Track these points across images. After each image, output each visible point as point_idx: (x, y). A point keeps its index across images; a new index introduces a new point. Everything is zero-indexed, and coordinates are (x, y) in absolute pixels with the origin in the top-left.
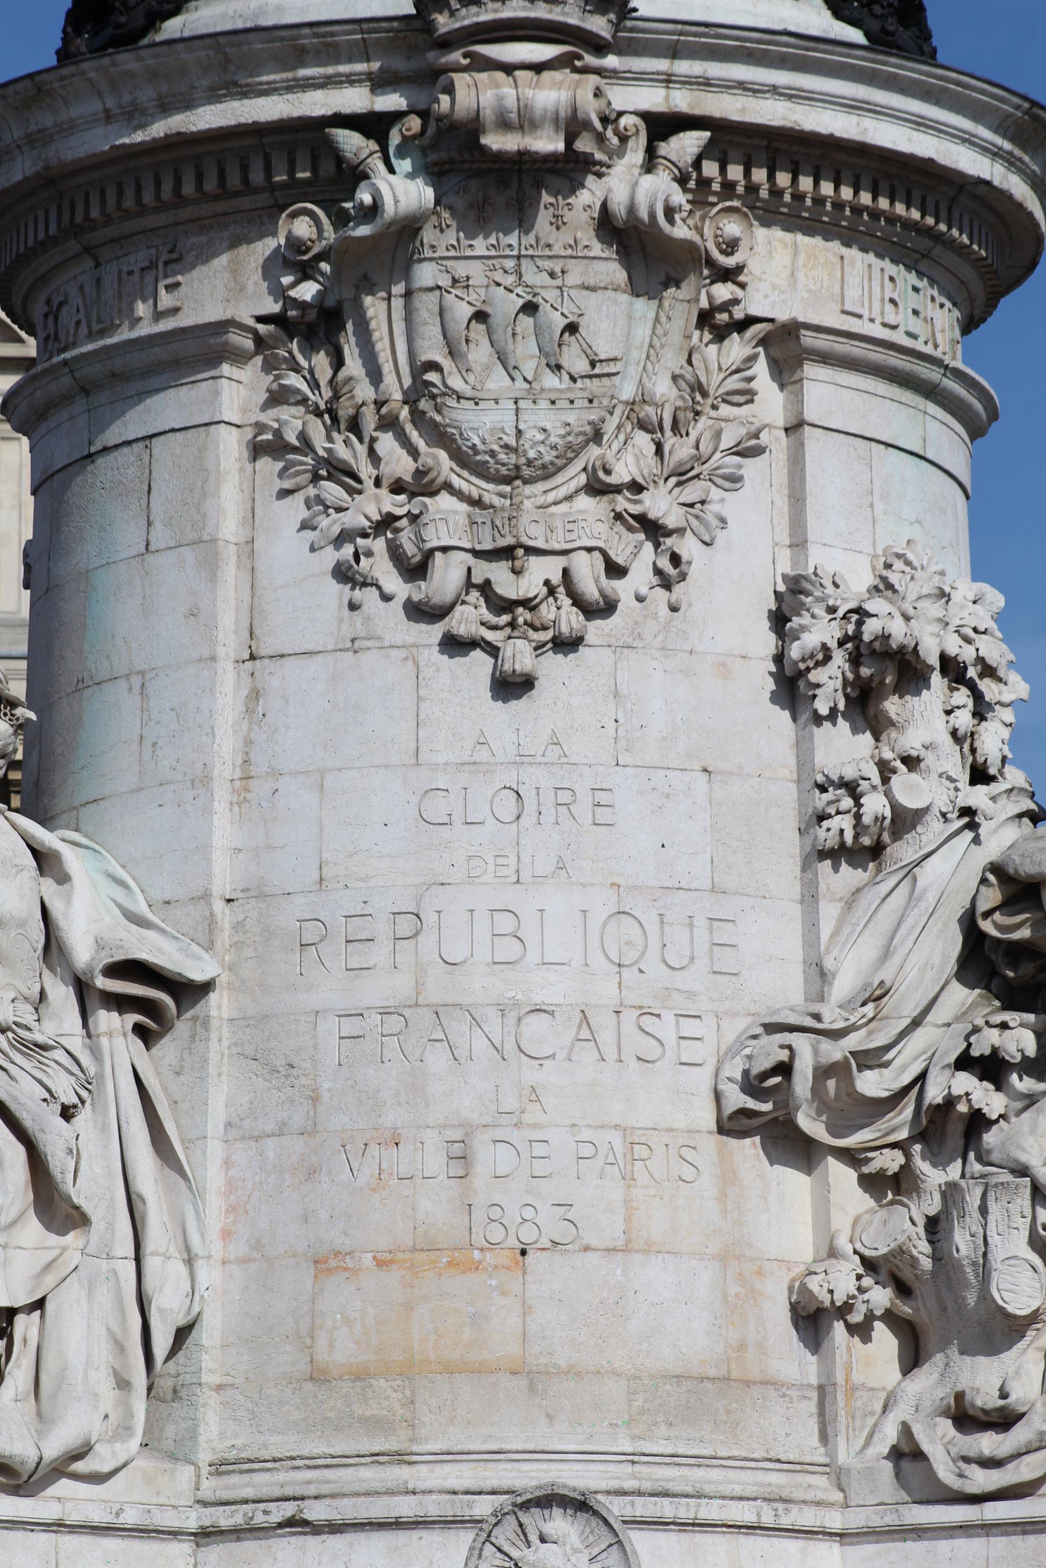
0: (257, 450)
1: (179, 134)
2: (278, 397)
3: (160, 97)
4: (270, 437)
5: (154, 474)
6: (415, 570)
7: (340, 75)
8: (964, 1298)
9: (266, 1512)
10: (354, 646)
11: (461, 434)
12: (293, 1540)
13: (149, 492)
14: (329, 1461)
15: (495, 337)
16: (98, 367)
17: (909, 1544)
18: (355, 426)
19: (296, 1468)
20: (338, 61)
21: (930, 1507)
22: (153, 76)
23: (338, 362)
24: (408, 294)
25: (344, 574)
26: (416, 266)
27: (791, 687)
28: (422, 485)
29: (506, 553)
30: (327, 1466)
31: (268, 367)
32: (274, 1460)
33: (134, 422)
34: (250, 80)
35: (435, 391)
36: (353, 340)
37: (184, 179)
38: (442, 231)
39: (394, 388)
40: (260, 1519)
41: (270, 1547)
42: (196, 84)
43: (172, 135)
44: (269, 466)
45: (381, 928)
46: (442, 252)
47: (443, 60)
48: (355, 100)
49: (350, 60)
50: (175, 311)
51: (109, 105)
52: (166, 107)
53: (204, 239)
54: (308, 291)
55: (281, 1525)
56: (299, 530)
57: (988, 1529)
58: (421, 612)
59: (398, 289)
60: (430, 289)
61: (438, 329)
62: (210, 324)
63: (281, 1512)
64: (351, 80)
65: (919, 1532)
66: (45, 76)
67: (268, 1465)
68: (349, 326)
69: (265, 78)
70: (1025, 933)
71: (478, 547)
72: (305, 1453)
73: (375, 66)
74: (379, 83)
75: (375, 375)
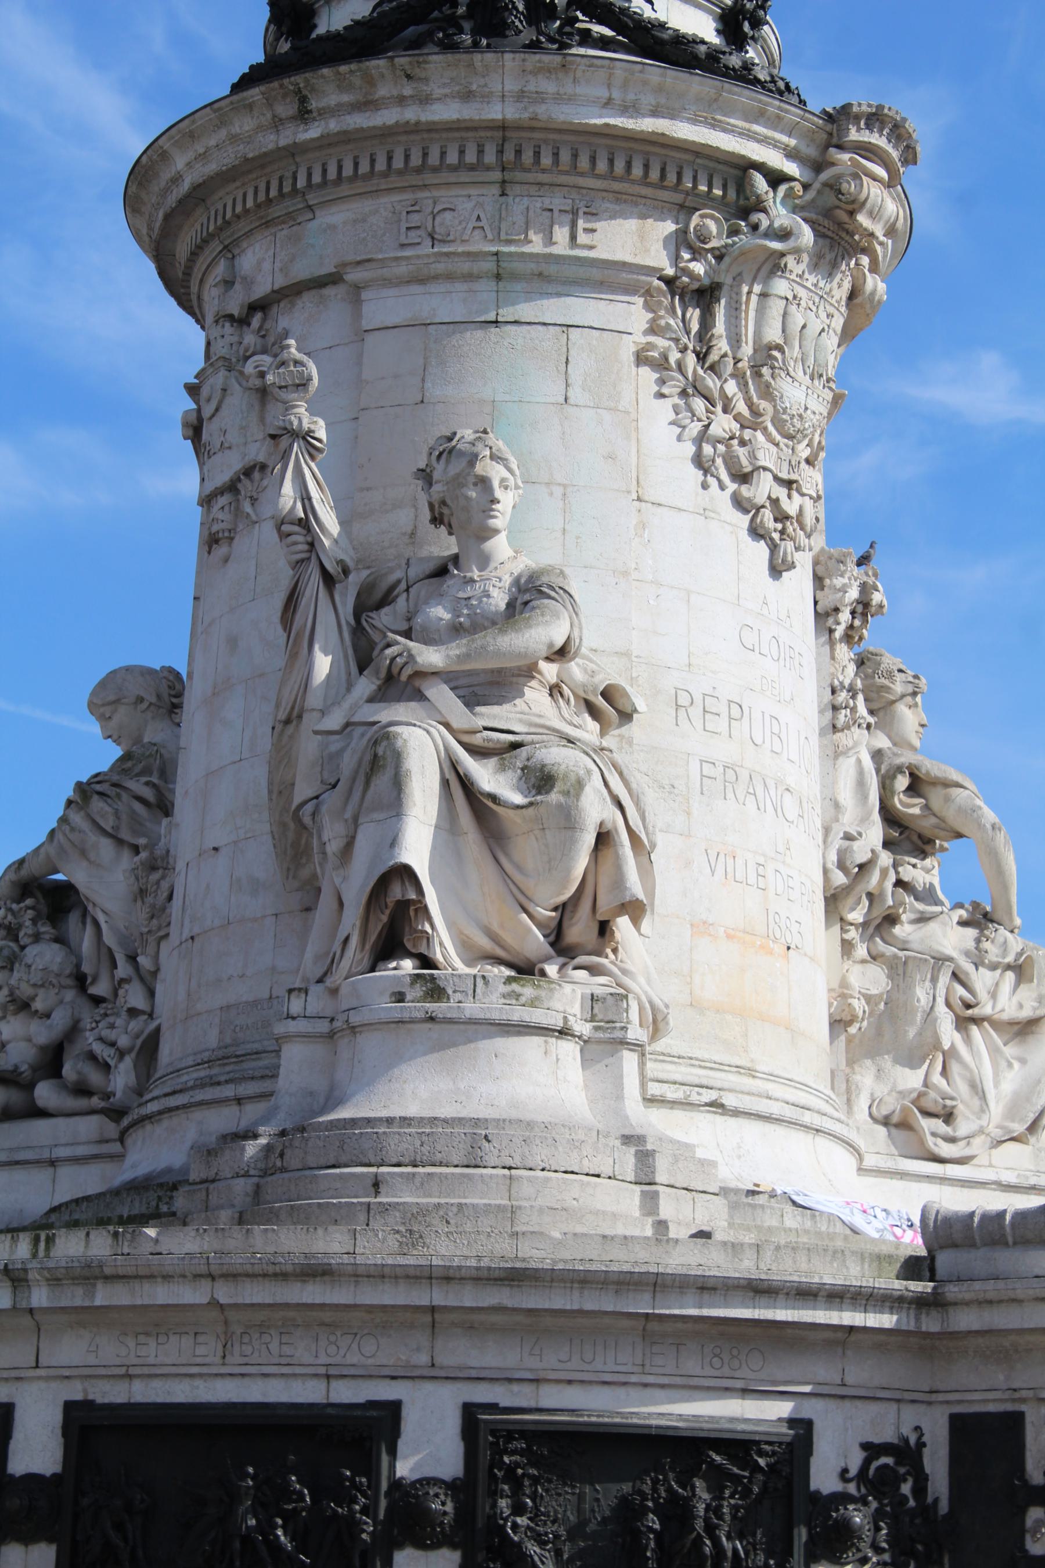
0: (641, 359)
1: (663, 134)
2: (653, 329)
3: (657, 106)
4: (656, 355)
5: (571, 352)
6: (743, 478)
7: (773, 139)
8: (906, 1032)
9: (699, 1094)
10: (705, 512)
11: (782, 397)
12: (708, 1115)
13: (567, 362)
14: (713, 1065)
15: (804, 343)
16: (533, 266)
17: (894, 1181)
18: (712, 368)
19: (693, 1065)
20: (775, 129)
21: (915, 1161)
22: (660, 89)
23: (707, 322)
24: (764, 295)
25: (699, 461)
26: (777, 279)
27: (824, 616)
28: (753, 421)
29: (789, 484)
30: (711, 1069)
31: (648, 307)
32: (679, 1057)
33: (525, 311)
34: (723, 118)
35: (776, 364)
36: (722, 311)
37: (634, 164)
38: (798, 263)
39: (747, 350)
40: (694, 1098)
41: (692, 1118)
42: (687, 107)
43: (657, 134)
44: (648, 376)
45: (723, 709)
46: (793, 277)
47: (839, 156)
48: (776, 160)
49: (782, 132)
50: (591, 248)
51: (613, 96)
52: (655, 113)
53: (617, 208)
54: (698, 268)
55: (706, 1105)
56: (670, 423)
57: (943, 1180)
58: (739, 503)
59: (757, 289)
60: (782, 298)
61: (779, 325)
62: (649, 267)
63: (708, 1096)
64: (775, 144)
65: (903, 1175)
66: (579, 59)
67: (676, 1060)
68: (723, 302)
69: (732, 121)
70: (916, 811)
71: (780, 475)
72: (700, 1057)
73: (793, 142)
74: (791, 154)
75: (736, 341)
